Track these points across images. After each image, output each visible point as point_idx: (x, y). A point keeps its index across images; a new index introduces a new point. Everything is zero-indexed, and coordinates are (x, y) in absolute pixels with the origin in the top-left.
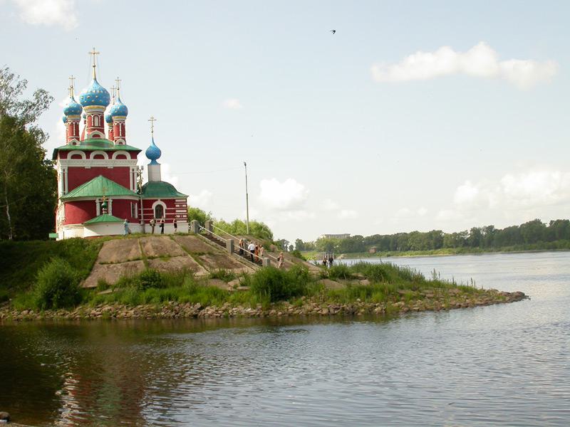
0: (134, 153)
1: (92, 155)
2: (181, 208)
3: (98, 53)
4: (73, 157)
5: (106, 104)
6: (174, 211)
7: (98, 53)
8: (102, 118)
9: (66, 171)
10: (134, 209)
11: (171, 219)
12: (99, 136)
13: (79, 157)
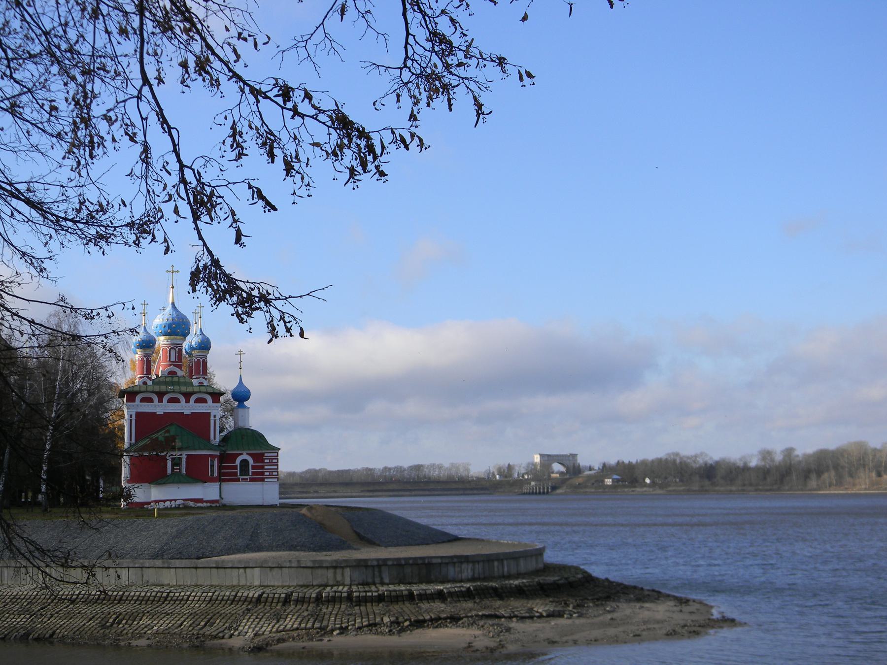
0: (216, 395)
1: (165, 398)
2: (271, 463)
3: (178, 271)
4: (143, 400)
5: (185, 335)
6: (262, 467)
7: (178, 271)
8: (180, 351)
9: (134, 417)
10: (212, 466)
11: (259, 477)
12: (175, 373)
13: (150, 400)
